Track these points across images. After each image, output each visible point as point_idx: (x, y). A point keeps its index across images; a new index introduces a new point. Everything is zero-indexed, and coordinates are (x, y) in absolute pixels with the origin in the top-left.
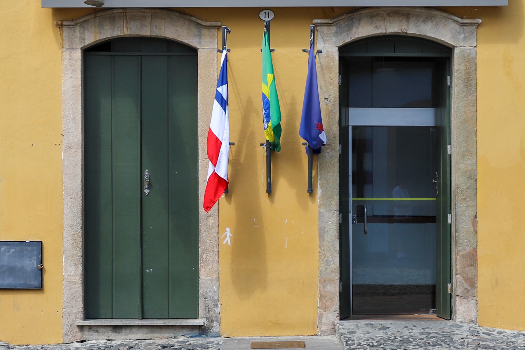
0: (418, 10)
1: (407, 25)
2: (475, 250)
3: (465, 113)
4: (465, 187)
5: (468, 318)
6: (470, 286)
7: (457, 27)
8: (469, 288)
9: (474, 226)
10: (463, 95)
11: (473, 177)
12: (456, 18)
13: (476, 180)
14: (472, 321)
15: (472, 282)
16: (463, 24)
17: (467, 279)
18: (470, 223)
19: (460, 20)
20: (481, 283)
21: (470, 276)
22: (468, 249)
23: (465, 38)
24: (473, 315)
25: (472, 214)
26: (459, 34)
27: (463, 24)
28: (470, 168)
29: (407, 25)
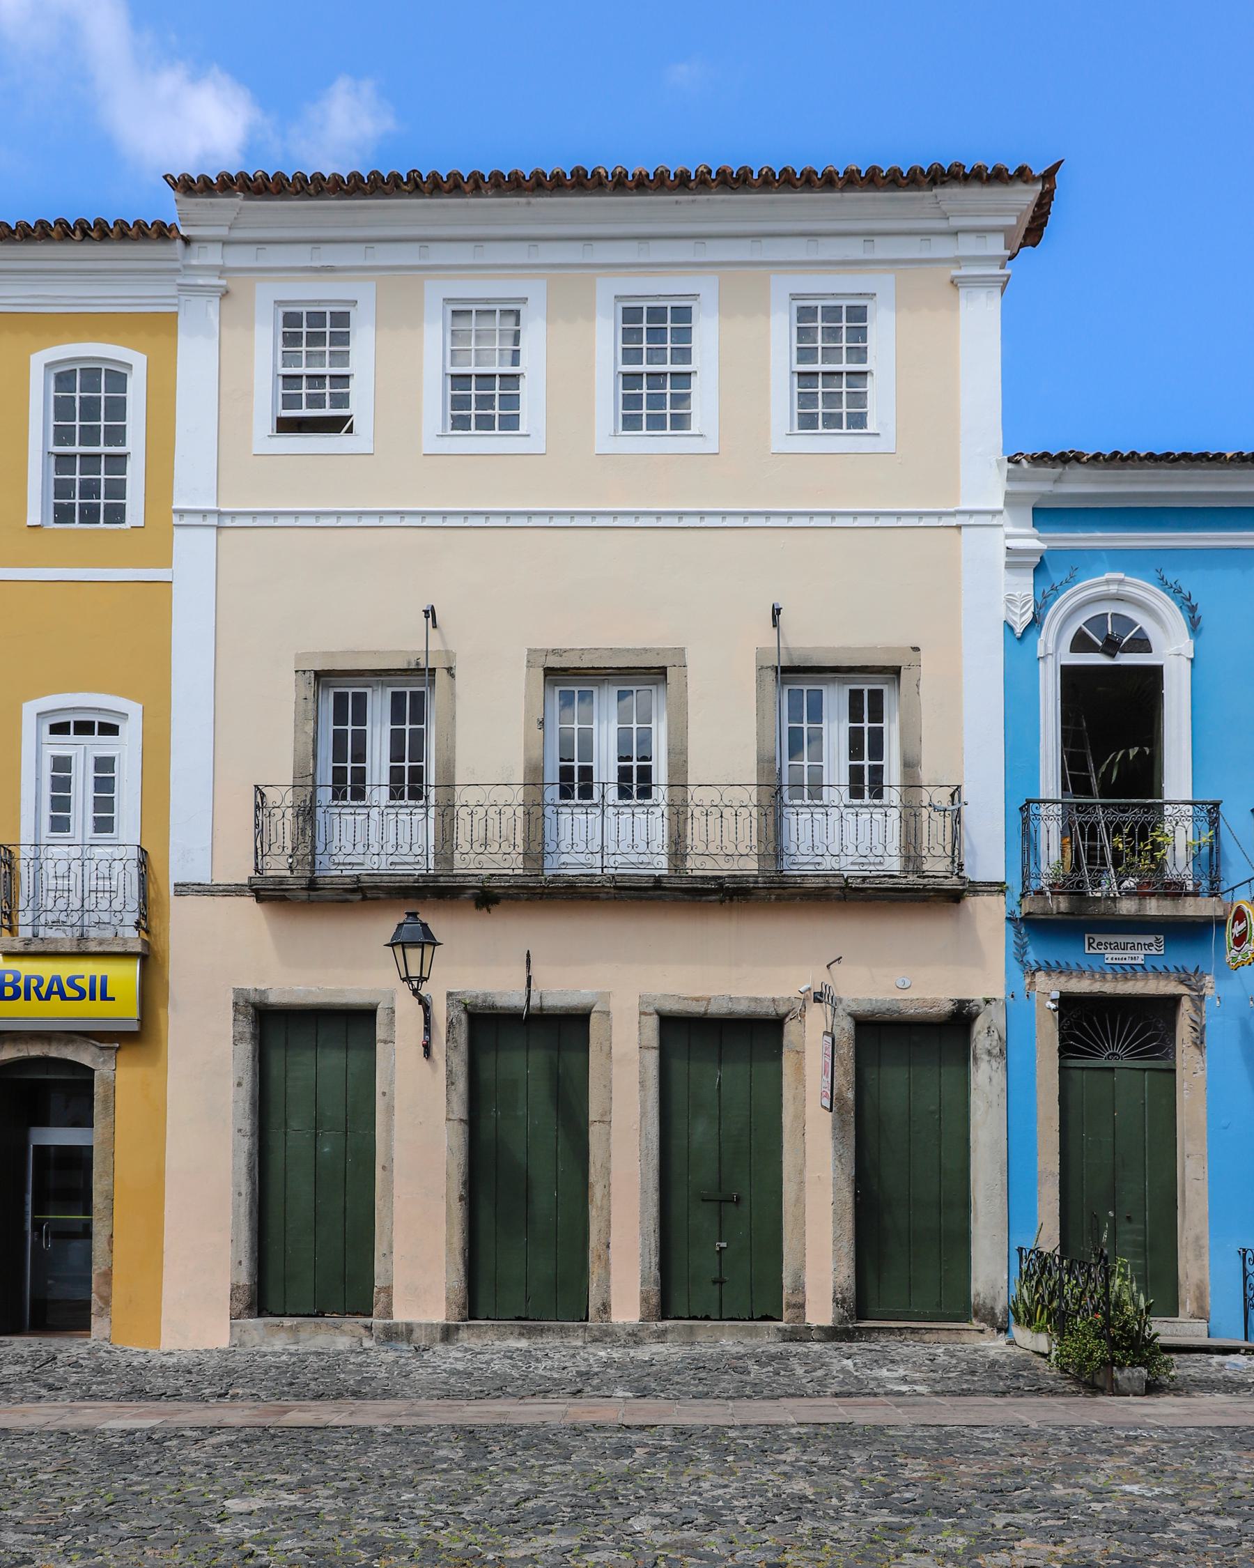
0: (58, 1034)
1: (49, 1049)
2: (110, 1269)
3: (103, 1134)
4: (102, 1207)
5: (102, 1337)
6: (104, 1304)
7: (97, 1051)
8: (103, 1306)
9: (109, 1245)
10: (101, 1116)
11: (110, 1199)
12: (94, 1042)
13: (113, 1200)
14: (106, 1339)
15: (107, 1301)
16: (102, 1048)
17: (101, 1297)
18: (106, 1245)
19: (98, 1044)
20: (115, 1301)
21: (105, 1294)
22: (104, 1268)
23: (104, 1062)
24: (107, 1333)
25: (108, 1233)
26: (99, 1057)
27: (102, 1048)
28: (107, 1188)
29: (49, 1049)
